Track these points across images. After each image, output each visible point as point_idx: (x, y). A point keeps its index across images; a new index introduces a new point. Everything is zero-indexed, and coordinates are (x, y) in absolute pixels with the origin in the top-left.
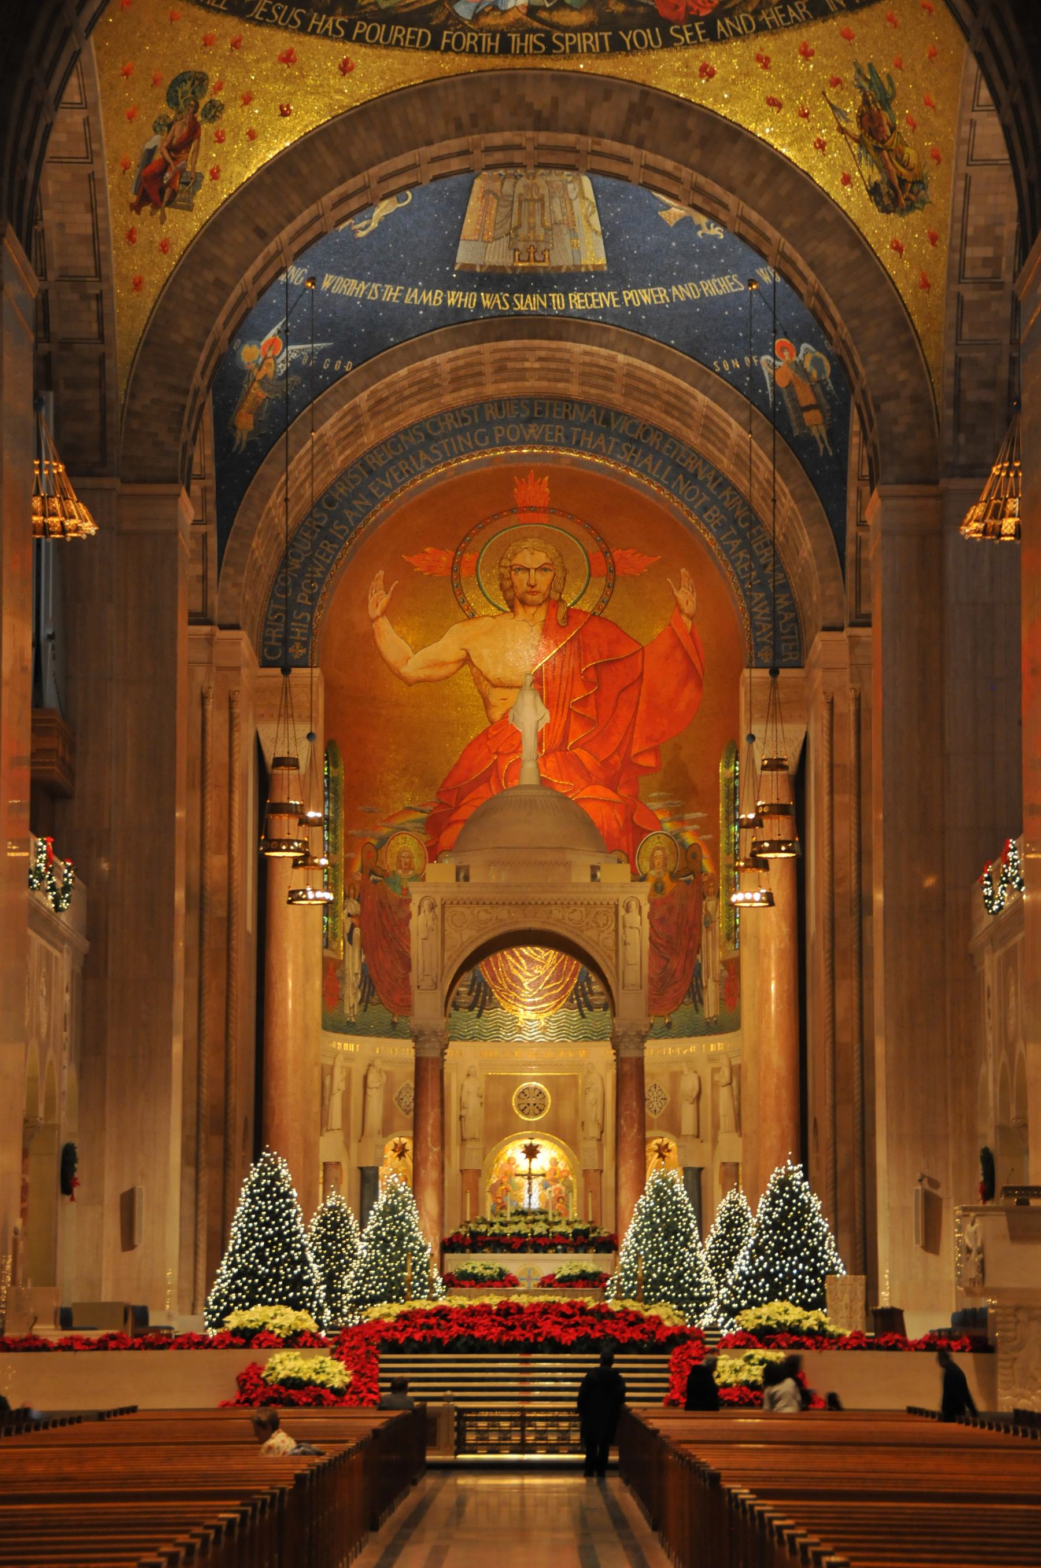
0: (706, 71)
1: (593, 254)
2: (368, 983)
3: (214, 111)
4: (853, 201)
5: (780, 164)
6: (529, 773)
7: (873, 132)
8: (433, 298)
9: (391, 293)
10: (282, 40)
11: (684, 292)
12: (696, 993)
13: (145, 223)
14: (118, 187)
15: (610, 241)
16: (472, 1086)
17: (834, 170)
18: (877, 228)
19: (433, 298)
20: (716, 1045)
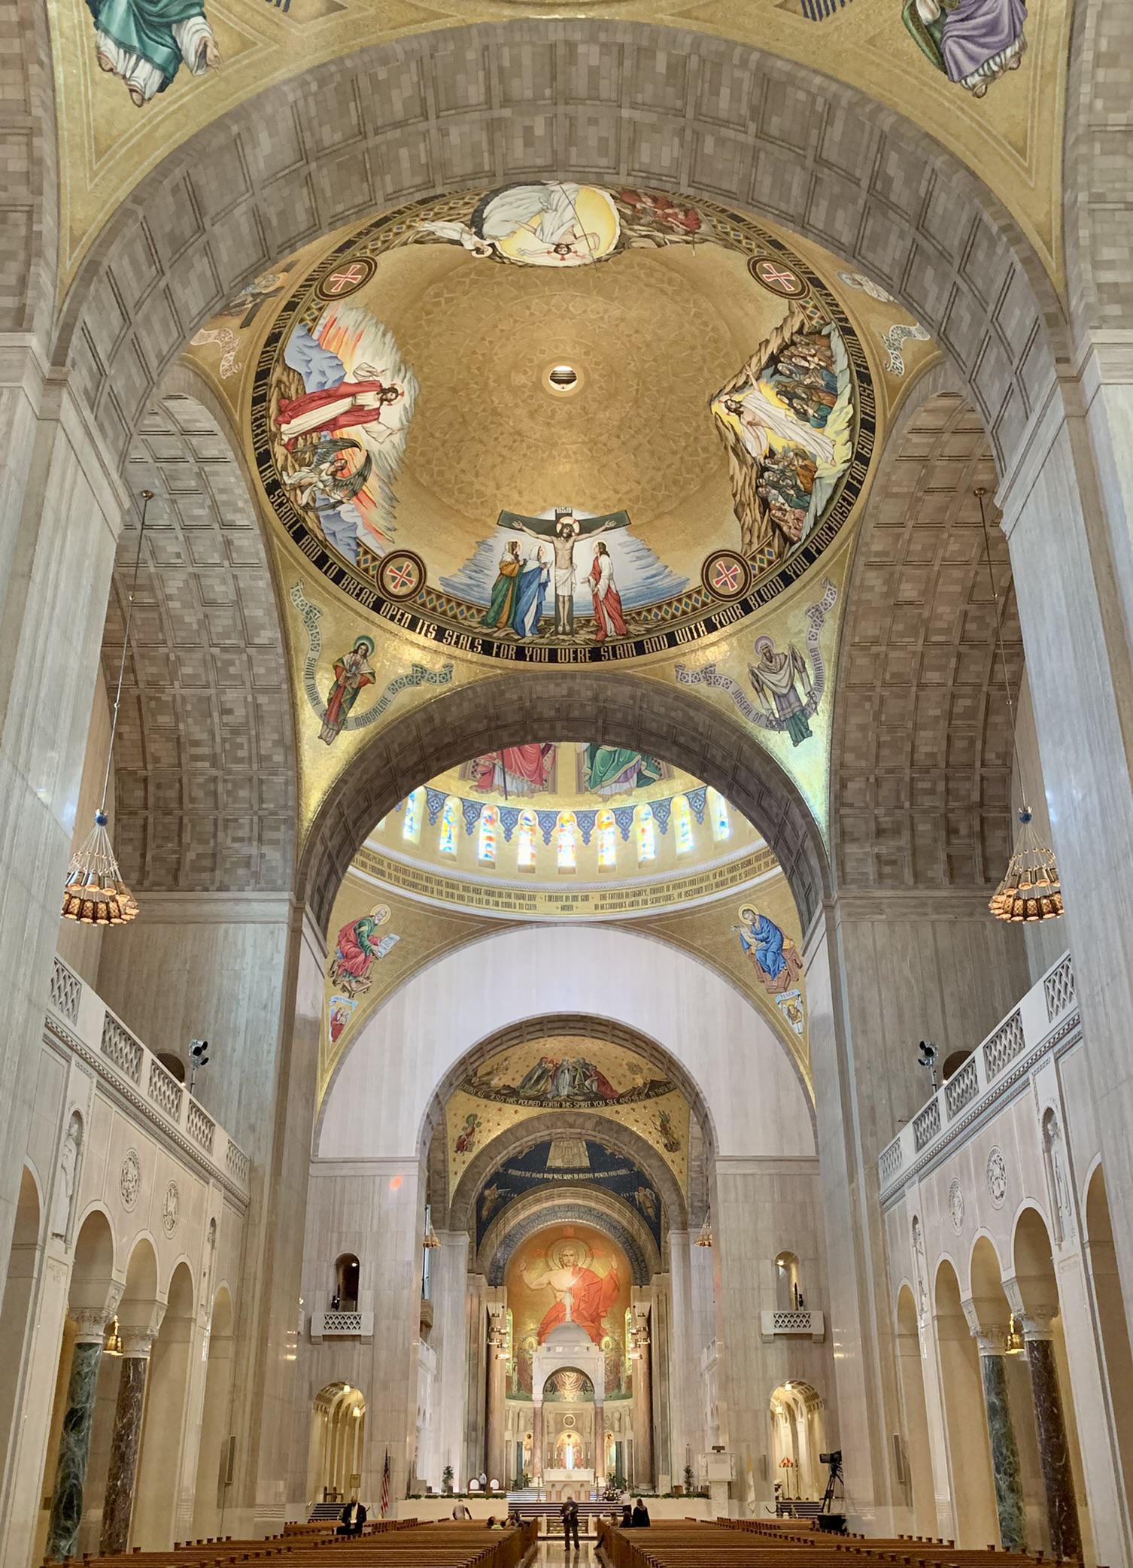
0: (617, 1112)
1: (586, 1163)
2: (519, 1384)
3: (479, 1124)
4: (660, 1148)
5: (639, 1137)
6: (568, 1318)
7: (665, 1129)
8: (540, 1176)
9: (528, 1174)
10: (499, 1105)
11: (612, 1174)
12: (619, 1386)
13: (459, 1156)
14: (451, 1146)
15: (591, 1157)
16: (551, 1416)
17: (655, 1140)
18: (667, 1156)
19: (540, 1176)
20: (625, 1402)
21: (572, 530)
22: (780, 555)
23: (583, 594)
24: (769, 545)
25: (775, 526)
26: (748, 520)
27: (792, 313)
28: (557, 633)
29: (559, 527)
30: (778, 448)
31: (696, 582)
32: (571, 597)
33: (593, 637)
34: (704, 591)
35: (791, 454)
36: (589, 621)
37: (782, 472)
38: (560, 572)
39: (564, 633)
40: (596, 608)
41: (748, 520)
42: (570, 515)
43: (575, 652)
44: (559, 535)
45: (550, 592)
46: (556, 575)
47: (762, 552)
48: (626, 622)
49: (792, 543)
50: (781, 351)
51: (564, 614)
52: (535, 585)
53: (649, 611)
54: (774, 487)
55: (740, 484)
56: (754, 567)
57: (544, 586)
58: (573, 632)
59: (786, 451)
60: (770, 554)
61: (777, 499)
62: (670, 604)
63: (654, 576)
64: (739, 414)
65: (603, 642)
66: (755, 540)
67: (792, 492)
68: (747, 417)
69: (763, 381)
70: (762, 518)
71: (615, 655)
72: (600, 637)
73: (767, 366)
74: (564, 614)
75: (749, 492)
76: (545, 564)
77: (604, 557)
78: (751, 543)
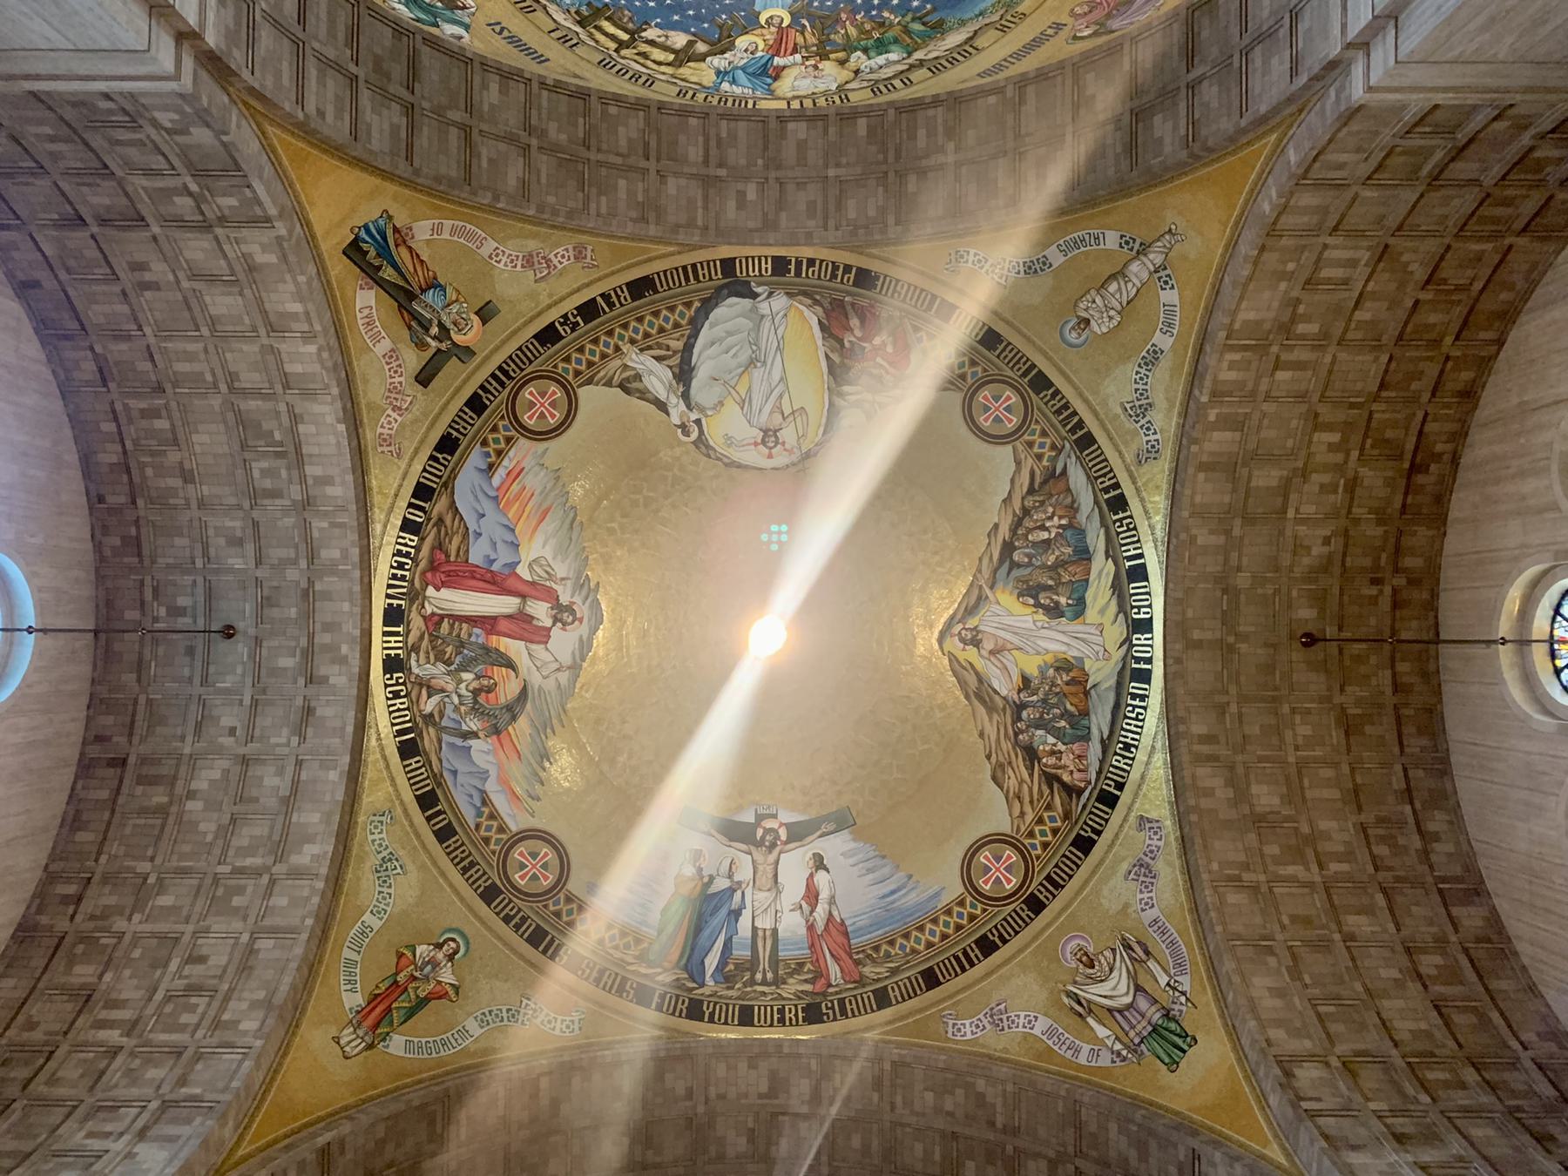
21: (777, 837)
22: (1067, 816)
23: (792, 925)
24: (1049, 807)
25: (1051, 779)
26: (1012, 783)
27: (1018, 463)
28: (752, 982)
29: (760, 832)
30: (1033, 671)
31: (956, 889)
32: (775, 931)
33: (808, 987)
34: (969, 899)
35: (1051, 671)
36: (801, 965)
37: (1044, 701)
38: (761, 895)
39: (764, 983)
40: (812, 946)
41: (1012, 783)
42: (775, 816)
43: (781, 1011)
44: (759, 844)
45: (744, 923)
46: (754, 899)
47: (1040, 821)
48: (857, 963)
49: (1080, 792)
50: (1014, 531)
51: (764, 954)
52: (723, 912)
53: (892, 943)
54: (1037, 727)
55: (993, 737)
56: (1034, 846)
57: (737, 914)
58: (778, 981)
59: (1042, 672)
60: (1052, 819)
61: (1045, 741)
62: (921, 929)
63: (893, 892)
64: (976, 643)
65: (824, 994)
66: (1028, 809)
67: (1063, 723)
68: (988, 645)
69: (1000, 585)
70: (1031, 775)
71: (844, 1013)
72: (819, 987)
73: (1001, 561)
74: (764, 954)
75: (1006, 746)
76: (740, 883)
77: (822, 873)
78: (1022, 814)
